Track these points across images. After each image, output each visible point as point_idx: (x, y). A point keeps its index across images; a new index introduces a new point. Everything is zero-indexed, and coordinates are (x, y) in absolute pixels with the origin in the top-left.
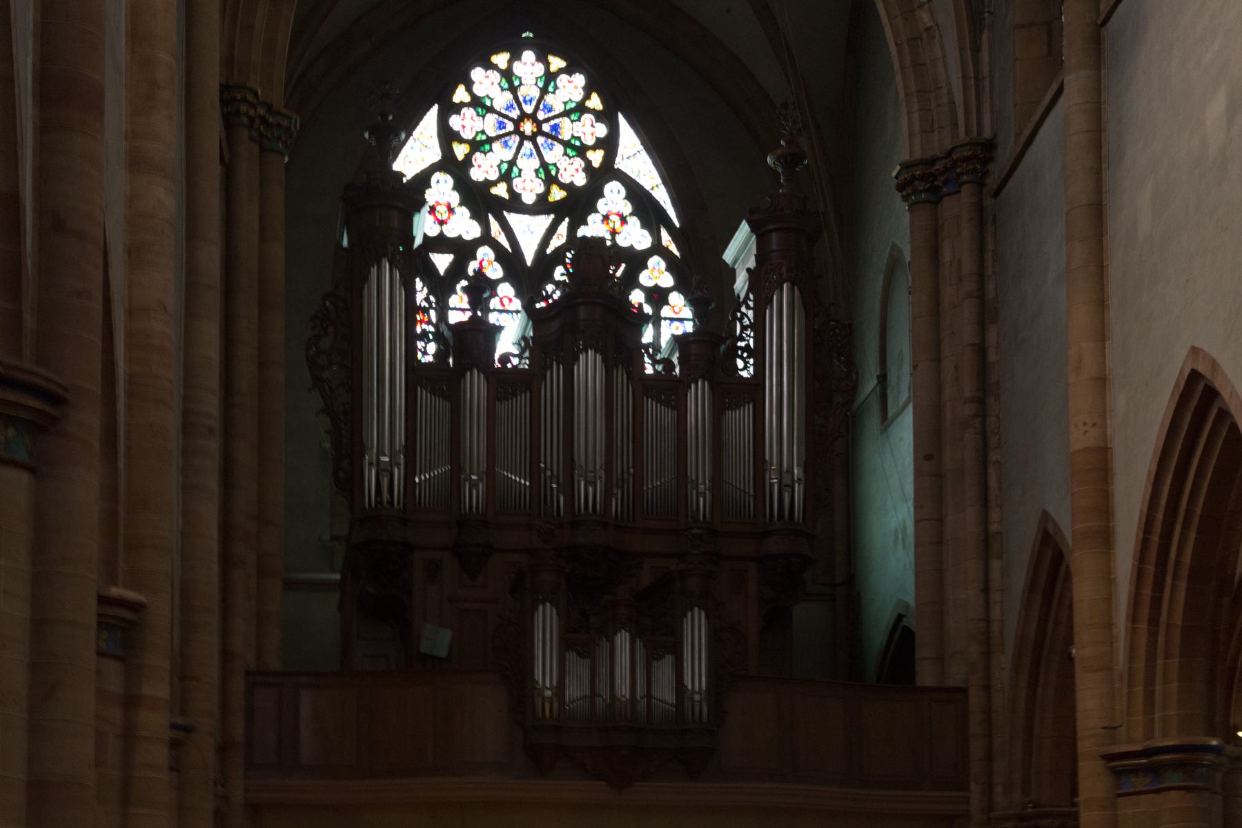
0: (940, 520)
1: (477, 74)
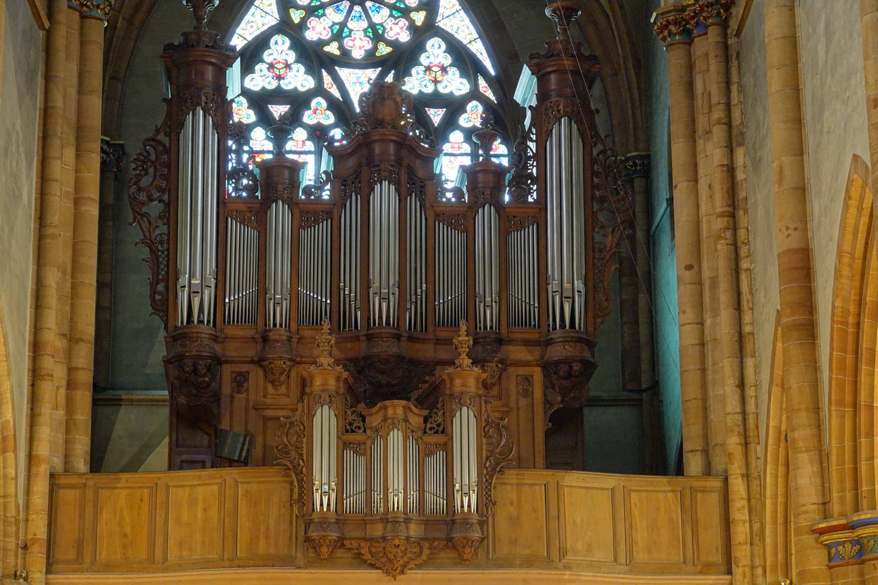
0: (702, 324)
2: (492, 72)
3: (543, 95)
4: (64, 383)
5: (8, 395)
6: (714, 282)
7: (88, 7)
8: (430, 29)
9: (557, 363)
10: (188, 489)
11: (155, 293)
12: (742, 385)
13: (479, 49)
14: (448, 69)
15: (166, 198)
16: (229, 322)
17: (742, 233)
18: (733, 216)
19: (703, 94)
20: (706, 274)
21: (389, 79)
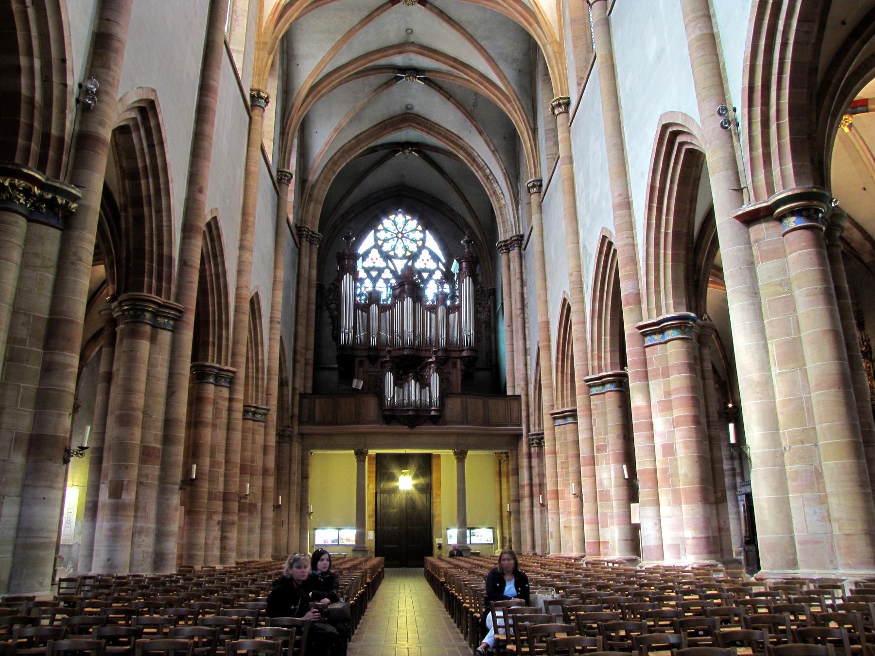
0: (513, 345)
2: (444, 261)
3: (460, 269)
6: (517, 330)
8: (423, 247)
17: (526, 315)
21: (410, 263)
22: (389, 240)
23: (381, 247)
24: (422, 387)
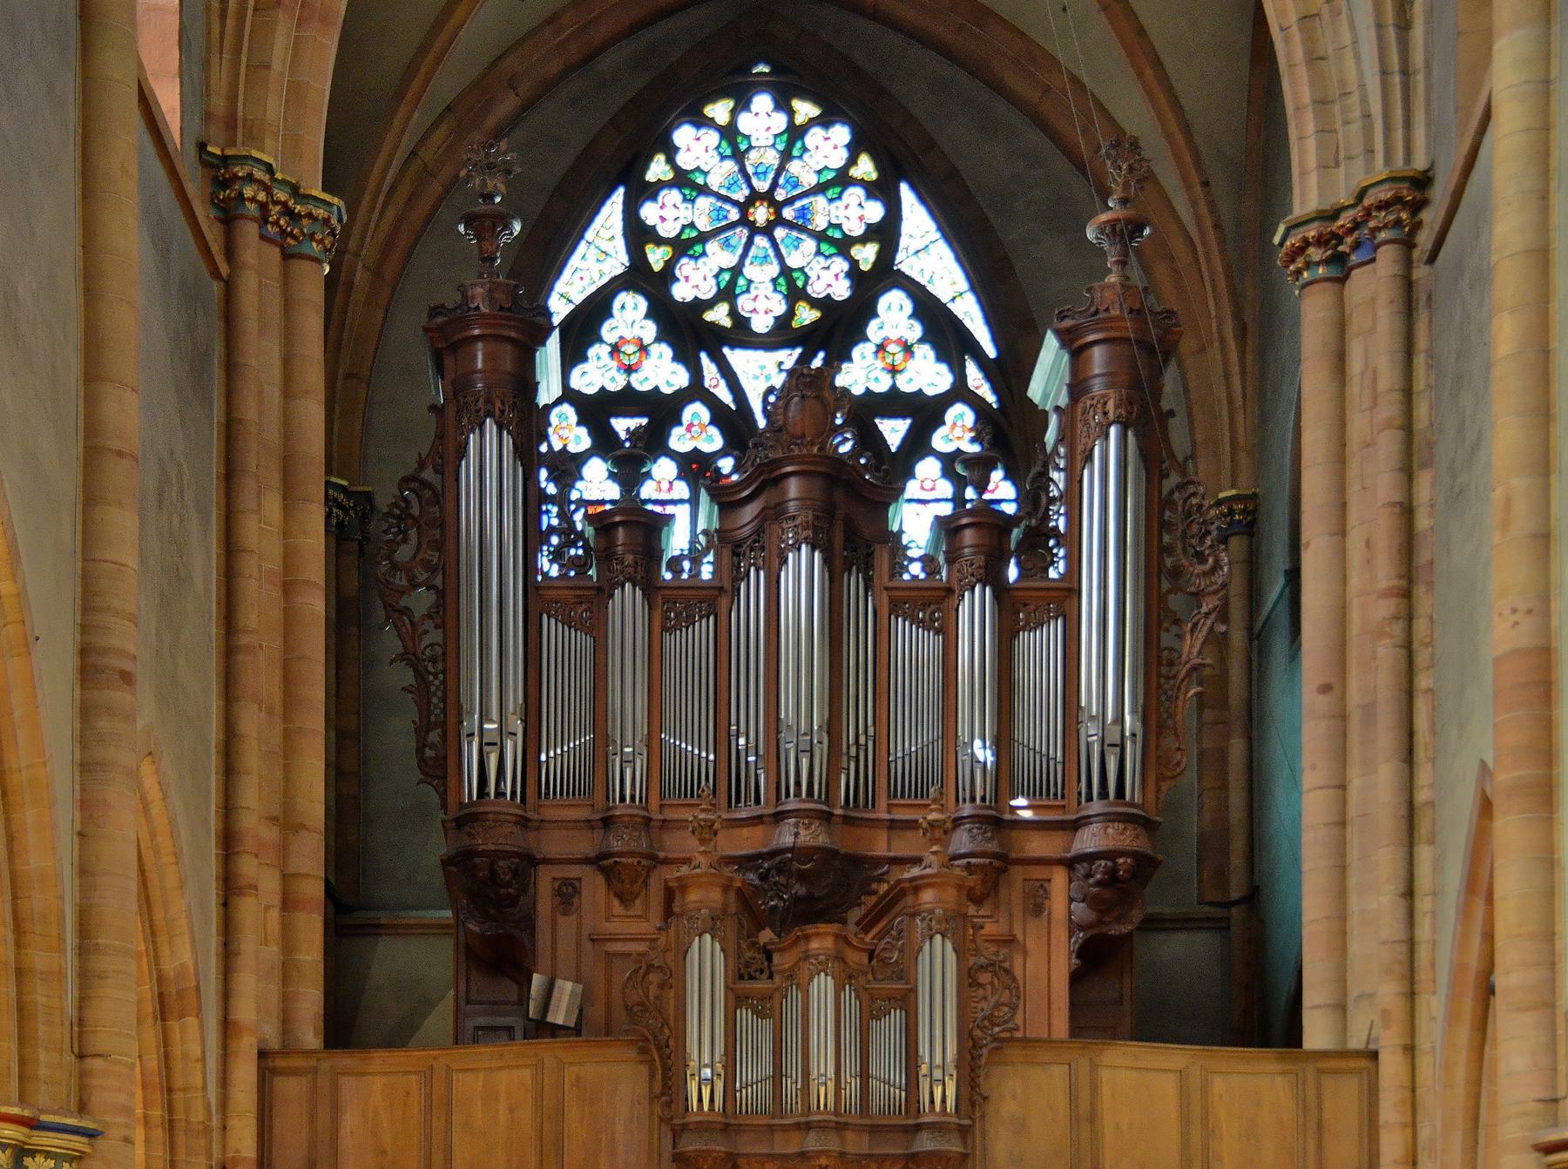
0: (1343, 787)
1: (684, 135)
2: (991, 352)
3: (1078, 388)
4: (276, 900)
5: (183, 922)
6: (1369, 710)
7: (295, 237)
8: (885, 275)
9: (1090, 858)
10: (481, 1075)
11: (424, 746)
12: (1409, 893)
13: (969, 313)
14: (915, 349)
15: (438, 581)
16: (547, 794)
17: (1421, 625)
18: (1407, 594)
19: (1362, 374)
20: (1355, 696)
22: (703, 238)
23: (668, 275)
24: (871, 1013)
